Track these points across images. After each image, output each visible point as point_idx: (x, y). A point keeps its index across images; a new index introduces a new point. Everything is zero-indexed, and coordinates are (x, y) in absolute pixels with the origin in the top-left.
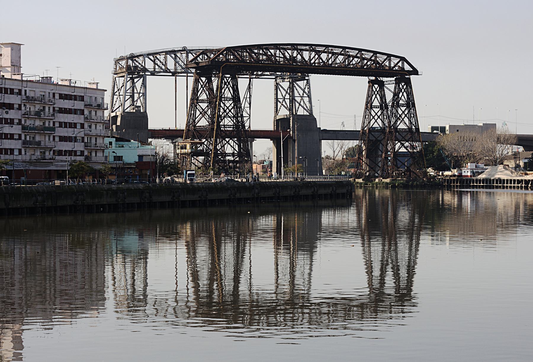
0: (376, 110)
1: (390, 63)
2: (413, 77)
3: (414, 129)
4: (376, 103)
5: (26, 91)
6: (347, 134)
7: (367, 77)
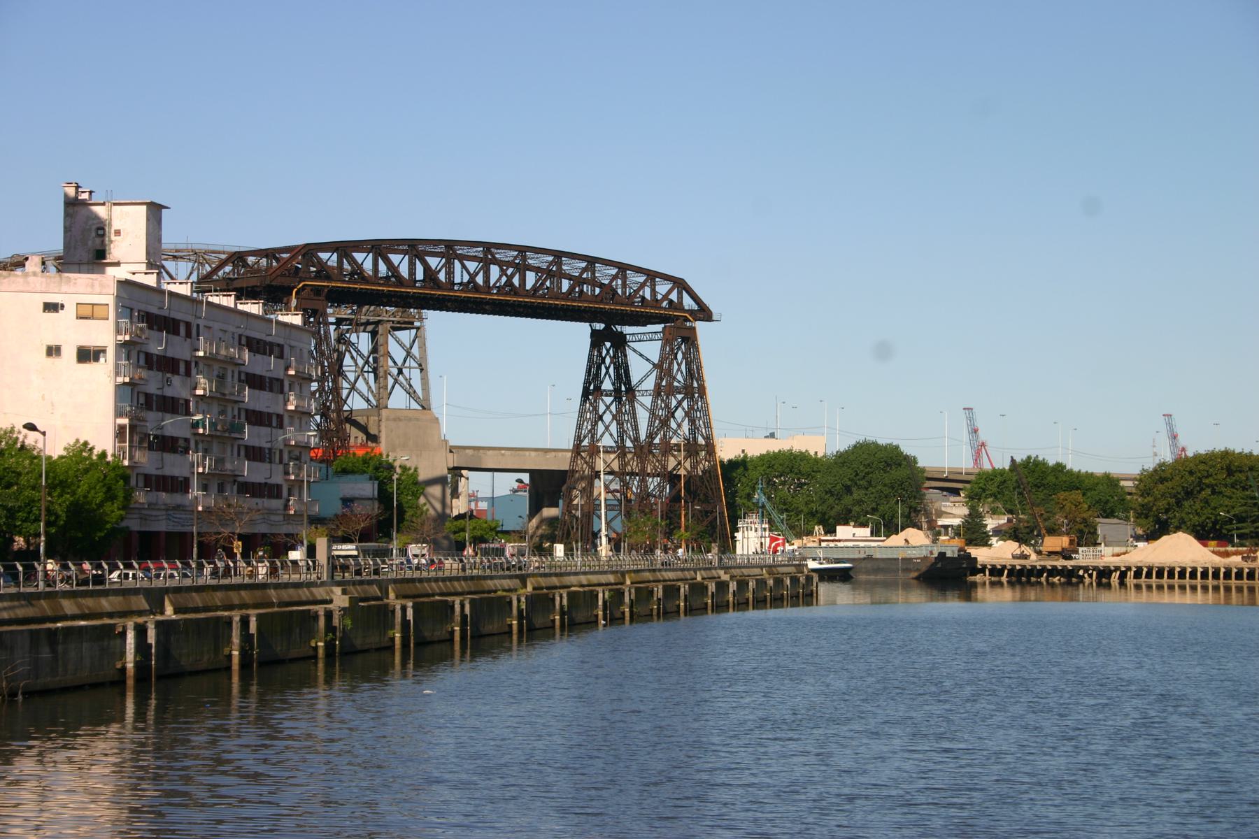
0: (608, 400)
1: (653, 292)
2: (700, 327)
4: (607, 385)
5: (198, 326)
6: (503, 455)
7: (588, 324)
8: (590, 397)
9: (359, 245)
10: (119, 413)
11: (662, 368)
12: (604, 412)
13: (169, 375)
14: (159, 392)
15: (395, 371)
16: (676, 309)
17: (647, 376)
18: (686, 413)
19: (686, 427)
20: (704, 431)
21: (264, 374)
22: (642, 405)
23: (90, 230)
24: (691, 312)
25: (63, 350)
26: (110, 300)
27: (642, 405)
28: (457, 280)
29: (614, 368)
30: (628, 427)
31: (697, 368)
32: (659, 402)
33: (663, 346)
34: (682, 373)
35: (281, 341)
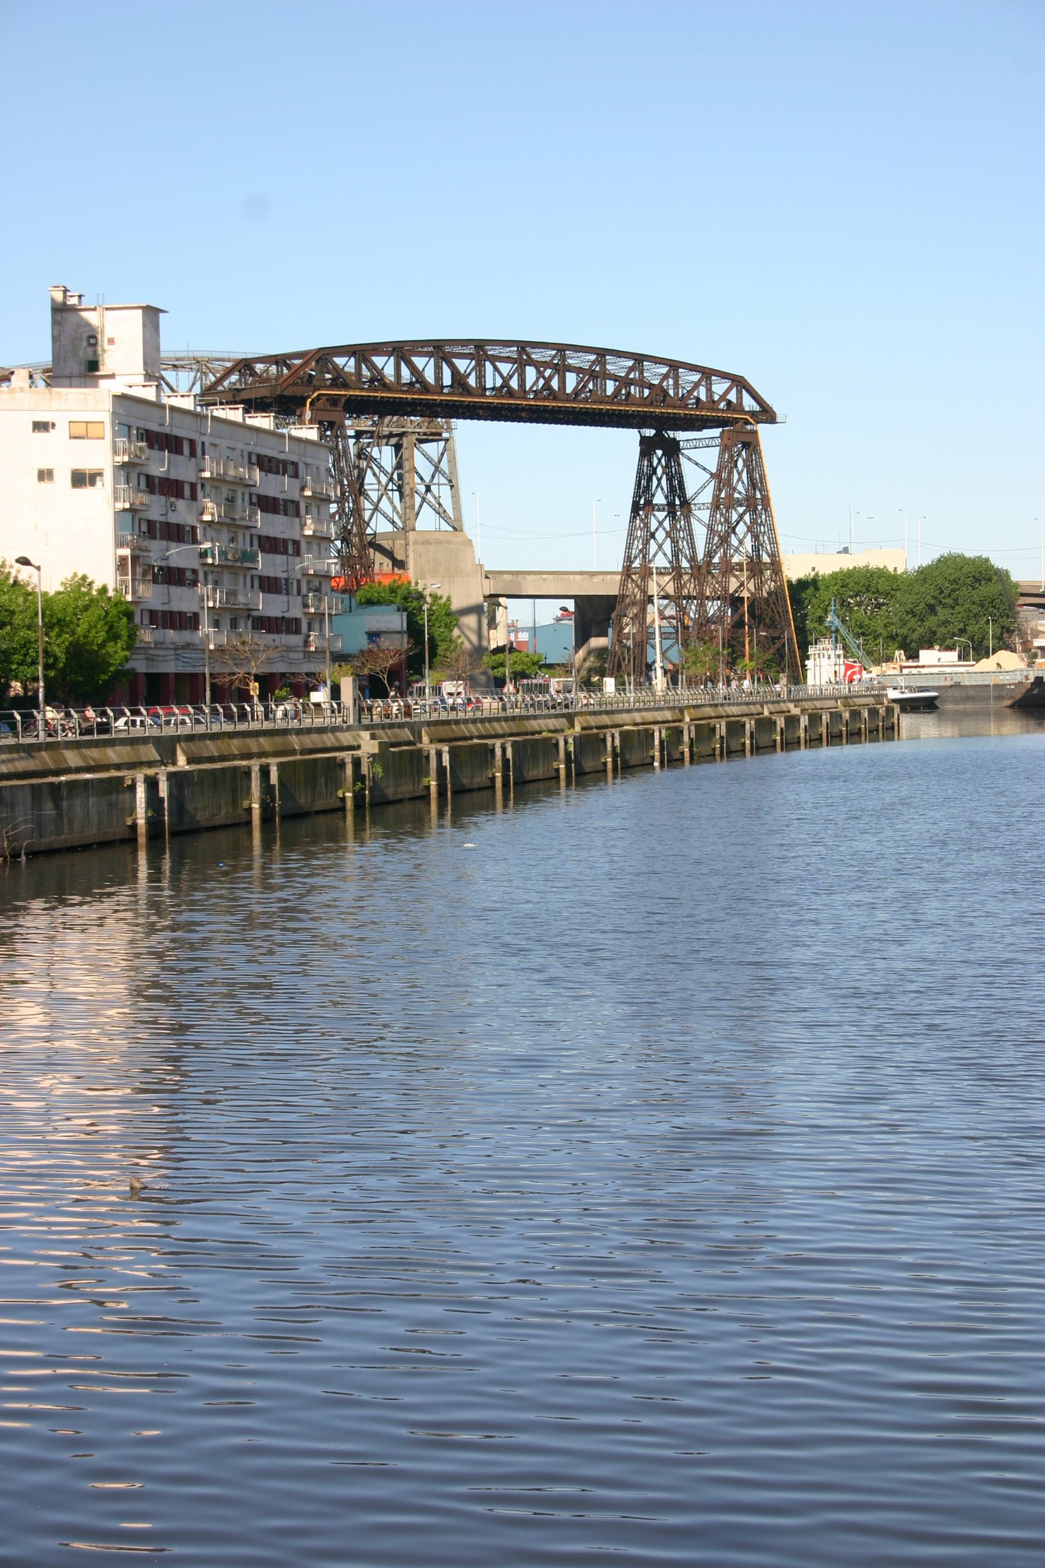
0: (661, 515)
2: (763, 430)
3: (765, 564)
4: (659, 499)
5: (203, 444)
6: (545, 580)
8: (641, 513)
9: (378, 348)
10: (120, 543)
11: (721, 478)
12: (657, 529)
13: (173, 499)
14: (163, 519)
15: (422, 489)
16: (735, 411)
17: (703, 487)
18: (748, 527)
19: (748, 543)
20: (769, 547)
21: (278, 495)
22: (699, 520)
23: (80, 339)
24: (752, 413)
25: (56, 474)
26: (106, 417)
27: (699, 520)
28: (489, 384)
29: (667, 479)
30: (683, 545)
31: (760, 477)
32: (718, 516)
33: (722, 453)
34: (743, 483)
35: (295, 459)
